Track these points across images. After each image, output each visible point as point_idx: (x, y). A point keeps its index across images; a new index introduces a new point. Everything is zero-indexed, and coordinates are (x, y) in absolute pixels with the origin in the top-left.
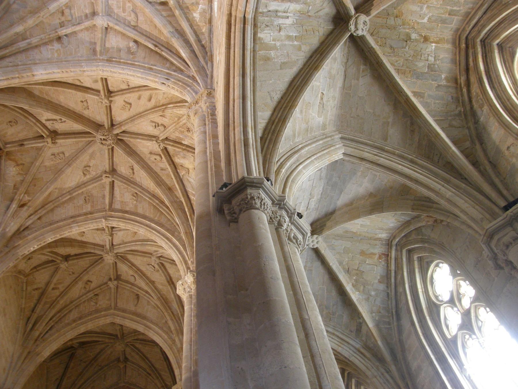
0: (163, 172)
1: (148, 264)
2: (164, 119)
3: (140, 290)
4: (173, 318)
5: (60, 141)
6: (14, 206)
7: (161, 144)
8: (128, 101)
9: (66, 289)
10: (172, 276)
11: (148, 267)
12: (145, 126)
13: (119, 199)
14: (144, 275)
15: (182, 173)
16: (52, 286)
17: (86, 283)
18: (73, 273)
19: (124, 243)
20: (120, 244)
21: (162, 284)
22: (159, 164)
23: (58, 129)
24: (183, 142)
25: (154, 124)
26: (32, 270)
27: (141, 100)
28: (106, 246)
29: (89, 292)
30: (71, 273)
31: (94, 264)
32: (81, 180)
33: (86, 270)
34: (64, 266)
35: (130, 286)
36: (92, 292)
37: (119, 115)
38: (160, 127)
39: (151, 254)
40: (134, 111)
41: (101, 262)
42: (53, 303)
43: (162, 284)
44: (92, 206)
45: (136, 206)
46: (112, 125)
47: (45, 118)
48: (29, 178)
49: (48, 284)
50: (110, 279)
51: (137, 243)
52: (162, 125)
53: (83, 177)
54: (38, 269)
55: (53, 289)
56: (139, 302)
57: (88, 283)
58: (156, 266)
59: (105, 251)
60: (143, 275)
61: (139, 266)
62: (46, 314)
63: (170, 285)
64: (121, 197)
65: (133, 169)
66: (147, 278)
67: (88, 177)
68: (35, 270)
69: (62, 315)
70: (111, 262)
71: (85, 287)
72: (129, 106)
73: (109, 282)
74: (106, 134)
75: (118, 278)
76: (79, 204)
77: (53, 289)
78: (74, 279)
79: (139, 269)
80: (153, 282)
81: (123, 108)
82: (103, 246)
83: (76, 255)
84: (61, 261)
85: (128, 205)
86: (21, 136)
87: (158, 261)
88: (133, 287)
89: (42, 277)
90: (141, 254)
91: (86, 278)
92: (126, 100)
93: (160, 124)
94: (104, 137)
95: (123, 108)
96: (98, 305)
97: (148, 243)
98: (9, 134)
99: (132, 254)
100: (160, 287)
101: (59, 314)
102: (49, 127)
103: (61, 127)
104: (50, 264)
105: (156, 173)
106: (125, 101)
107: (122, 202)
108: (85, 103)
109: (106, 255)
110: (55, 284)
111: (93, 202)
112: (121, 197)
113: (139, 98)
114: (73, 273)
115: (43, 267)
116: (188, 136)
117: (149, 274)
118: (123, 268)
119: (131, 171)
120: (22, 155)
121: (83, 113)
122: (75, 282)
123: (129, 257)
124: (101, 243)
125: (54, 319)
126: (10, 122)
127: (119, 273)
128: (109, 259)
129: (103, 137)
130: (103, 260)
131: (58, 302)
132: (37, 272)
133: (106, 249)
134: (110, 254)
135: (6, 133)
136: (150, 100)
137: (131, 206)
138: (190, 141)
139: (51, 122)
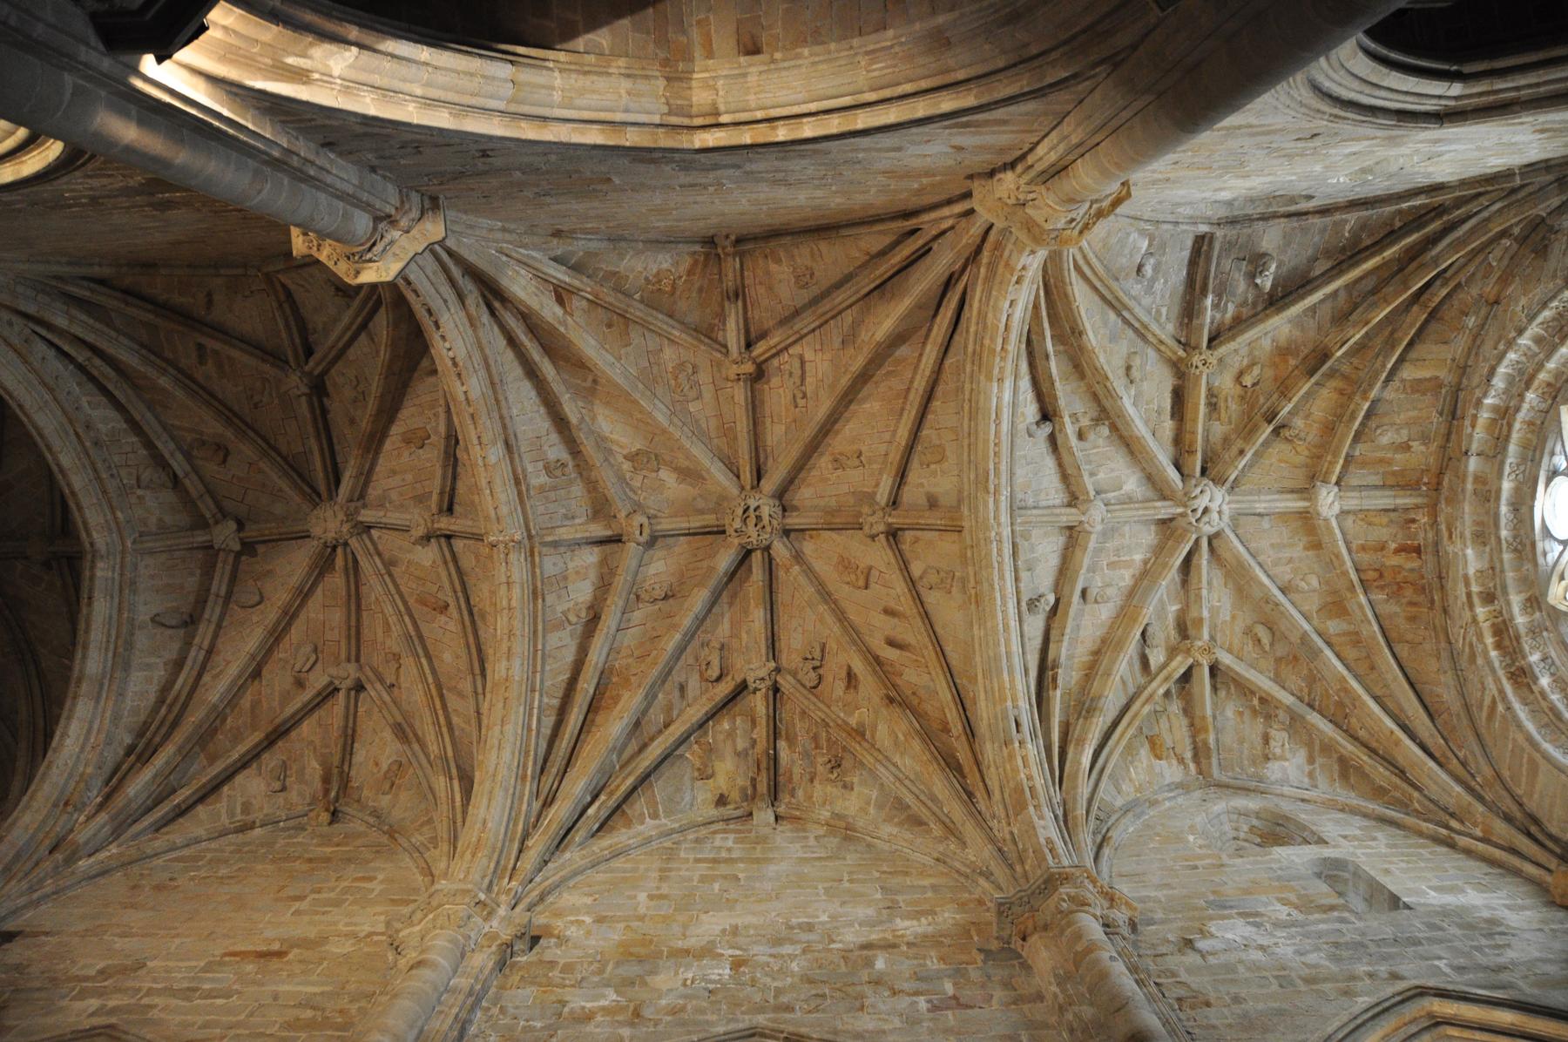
0: (677, 693)
1: (315, 650)
2: (840, 686)
3: (213, 627)
4: (159, 780)
5: (740, 393)
6: (560, 274)
7: (769, 683)
8: (872, 579)
9: (202, 387)
10: (293, 734)
11: (308, 648)
12: (805, 626)
13: (571, 565)
14: (278, 640)
15: (692, 754)
16: (211, 344)
17: (219, 447)
18: (256, 406)
19: (390, 564)
20: (379, 555)
21: (255, 705)
22: (696, 676)
23: (768, 382)
24: (782, 744)
25: (817, 654)
26: (284, 286)
27: (882, 617)
28: (365, 506)
29: (188, 456)
30: (256, 398)
31: (295, 469)
32: (615, 448)
33: (269, 447)
34: (295, 383)
35: (223, 592)
36: (188, 468)
37: (822, 552)
38: (813, 675)
39: (358, 660)
40: (842, 591)
41: (303, 493)
42: (154, 353)
43: (255, 705)
44: (542, 489)
45: (559, 626)
46: (787, 532)
47: (809, 355)
48: (637, 311)
49: (221, 331)
50: (241, 526)
51: (407, 619)
52: (820, 677)
53: (625, 452)
54: (286, 306)
55: (200, 347)
56: (170, 632)
57: (221, 454)
58: (318, 681)
59: (353, 505)
60: (277, 635)
61: (302, 616)
62: (121, 338)
63: (267, 737)
64: (577, 573)
65: (666, 598)
66: (270, 651)
67: (627, 466)
68: (282, 297)
69: (110, 387)
70: (317, 531)
71: (203, 443)
72: (861, 583)
73: (233, 525)
74: (775, 522)
75: (248, 548)
76: (546, 448)
77: (200, 347)
78: (236, 408)
79: (294, 616)
80: (256, 674)
81: (845, 565)
82: (362, 496)
83: (324, 412)
84: (310, 373)
85: (559, 597)
86: (757, 292)
87: (345, 685)
88: (221, 601)
89: (250, 314)
90: (353, 623)
91: (245, 450)
92: (874, 573)
93: (821, 671)
94: (766, 519)
95: (845, 565)
96: (140, 492)
97: (424, 661)
98: (773, 267)
99: (349, 596)
100: (246, 702)
101: (112, 374)
102: (775, 362)
103: (778, 393)
104: (297, 341)
105: (669, 673)
106: (870, 568)
107: (565, 578)
108: (857, 462)
109: (341, 516)
110: (216, 352)
111: (555, 488)
112: (577, 573)
113: (888, 612)
114: (256, 406)
115: (291, 319)
116: (813, 764)
117: (280, 654)
118: (293, 565)
119: (659, 593)
120: (700, 290)
121: (822, 454)
122: (229, 414)
123: (336, 580)
124: (373, 492)
125: (97, 362)
126: (812, 275)
127: (261, 549)
128: (328, 523)
129: (765, 512)
130: (316, 505)
131: (164, 372)
132: (275, 305)
133: (357, 511)
134: (345, 528)
135: (778, 261)
136: (891, 643)
137: (559, 609)
138: (797, 771)
139: (798, 372)
